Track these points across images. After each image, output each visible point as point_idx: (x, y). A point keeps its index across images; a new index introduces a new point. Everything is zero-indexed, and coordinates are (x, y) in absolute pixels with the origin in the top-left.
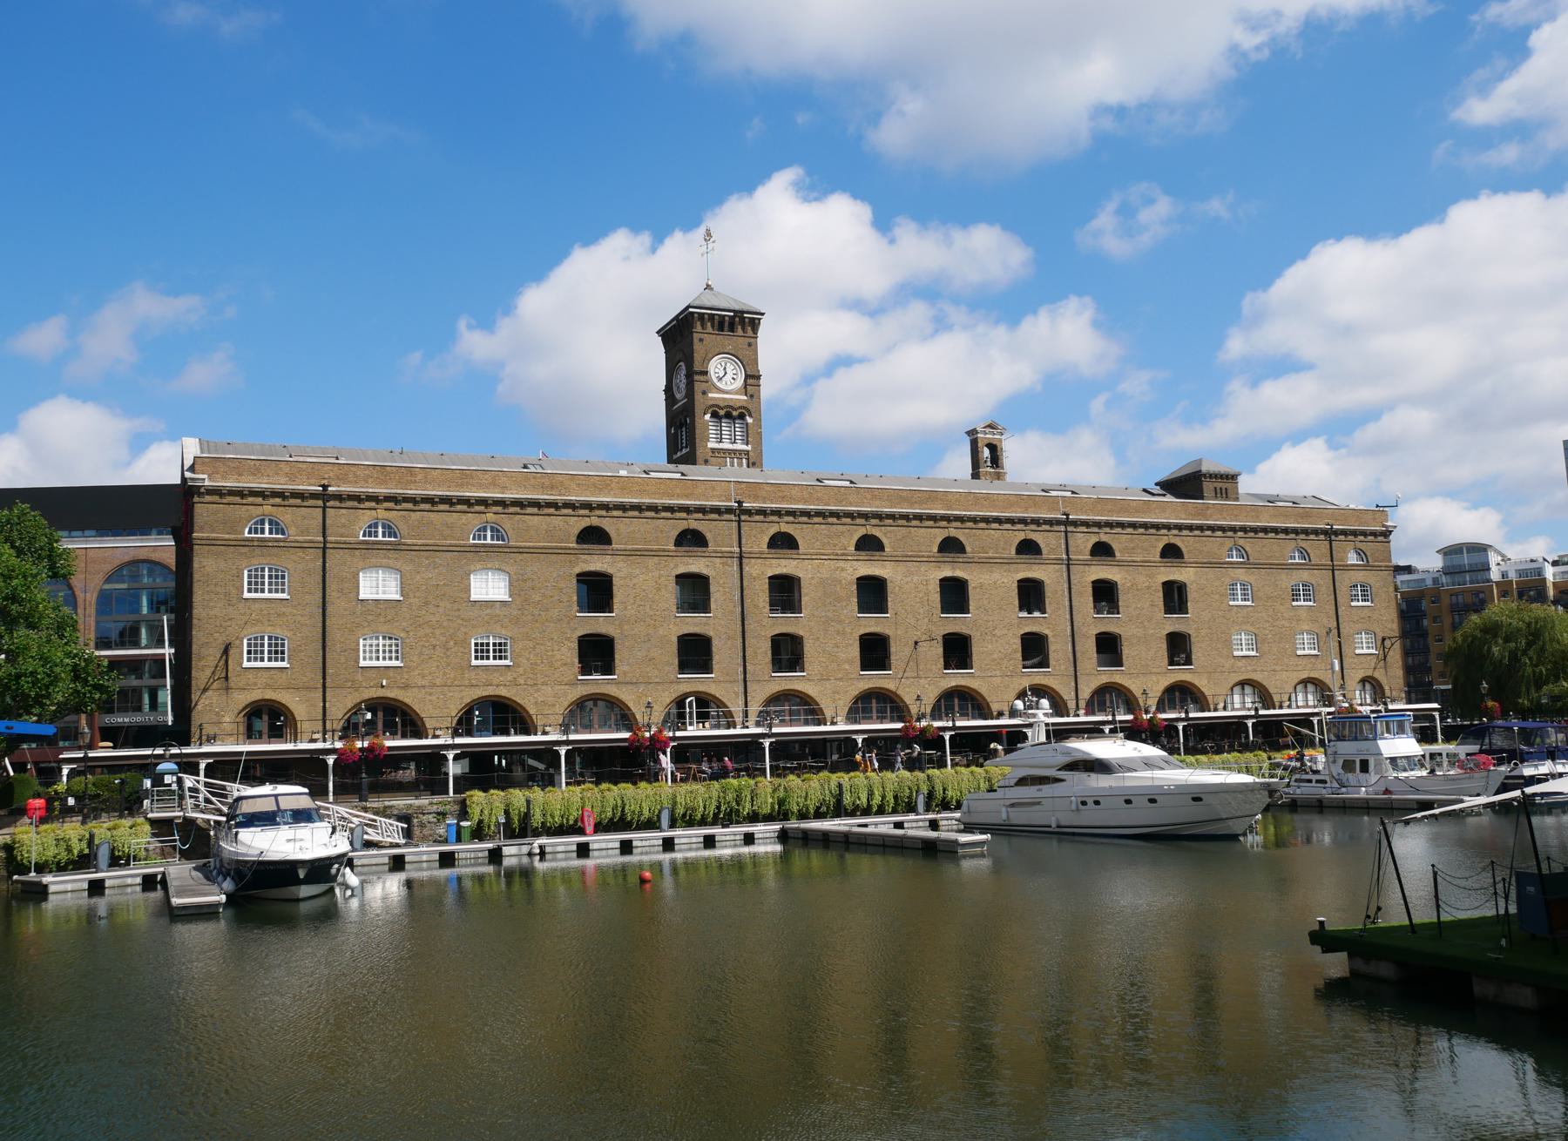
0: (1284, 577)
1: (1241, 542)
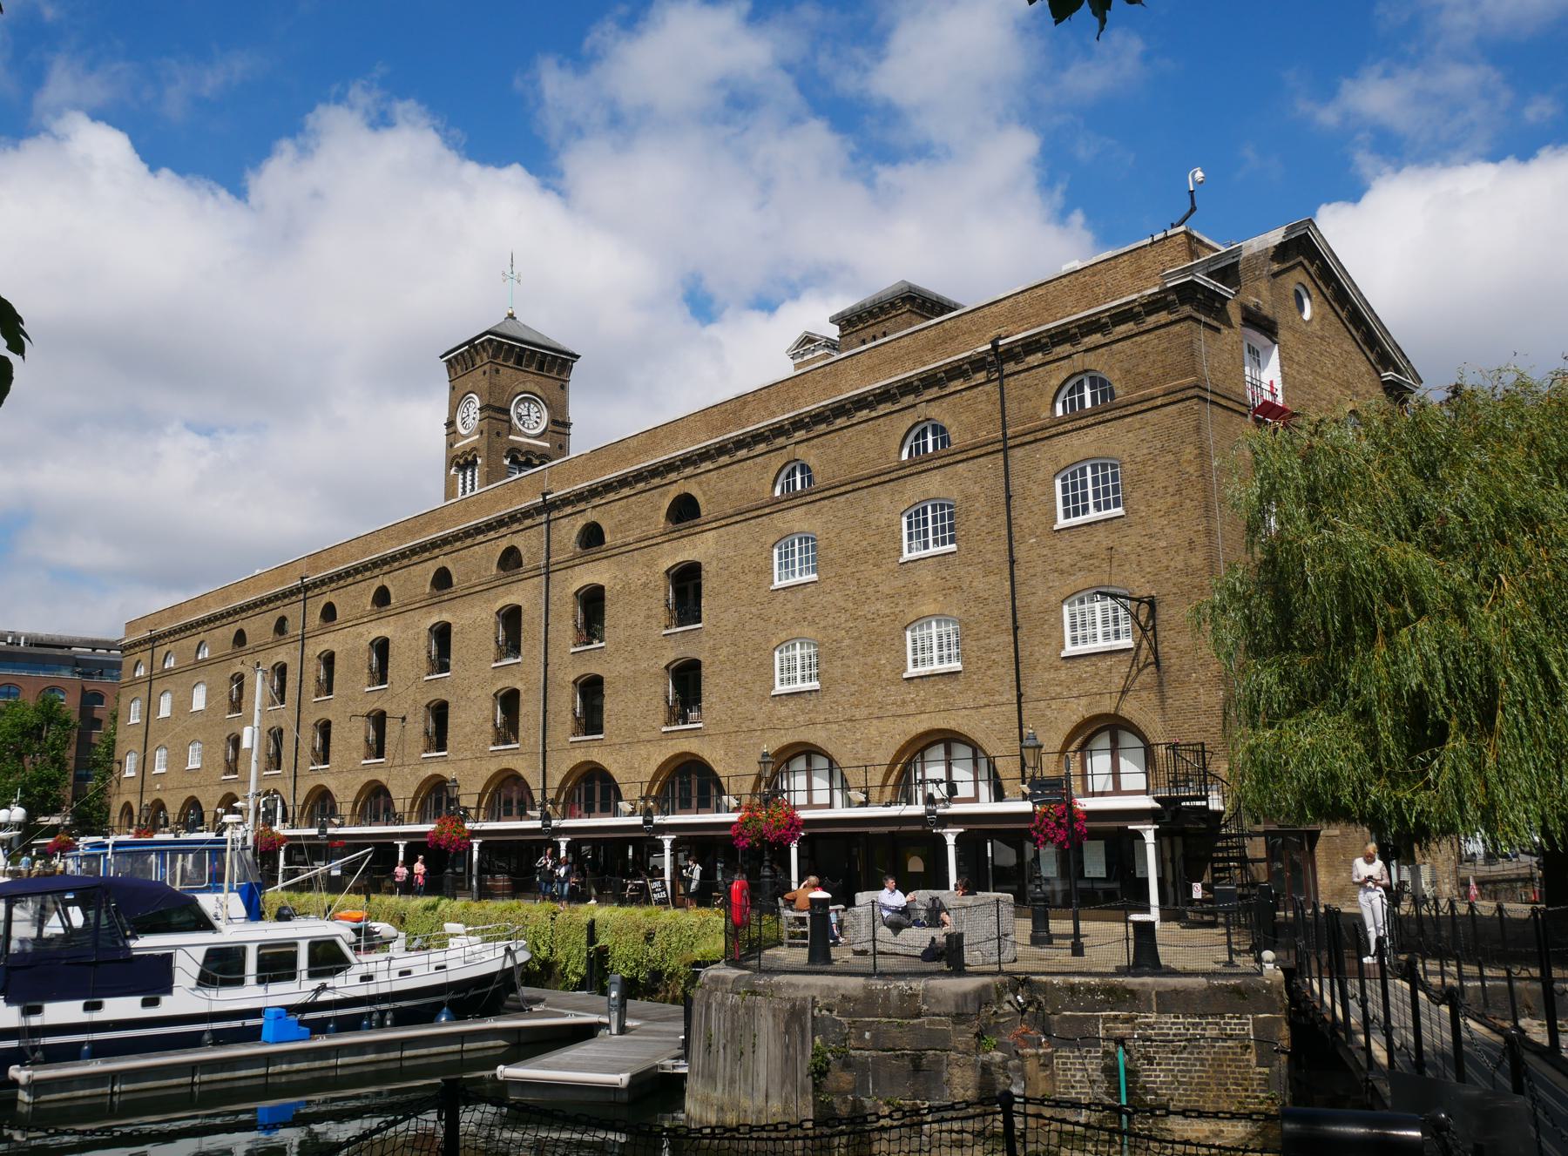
0: (885, 501)
1: (801, 452)
